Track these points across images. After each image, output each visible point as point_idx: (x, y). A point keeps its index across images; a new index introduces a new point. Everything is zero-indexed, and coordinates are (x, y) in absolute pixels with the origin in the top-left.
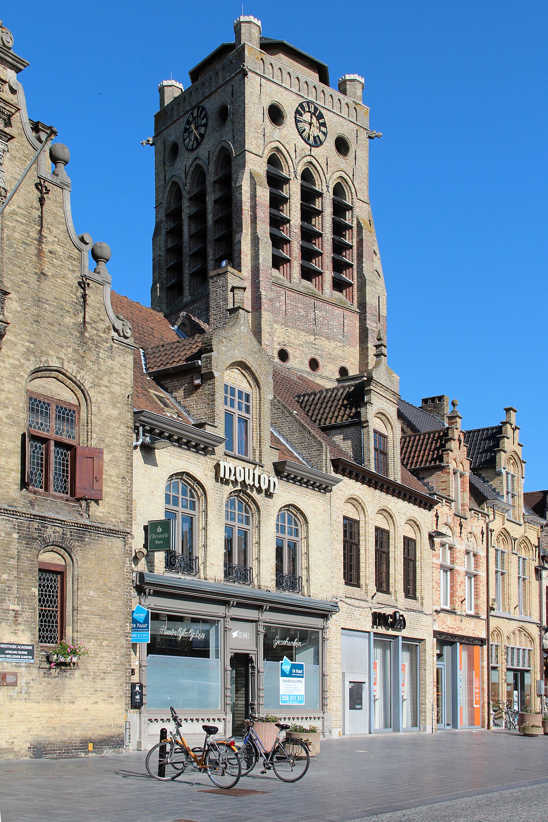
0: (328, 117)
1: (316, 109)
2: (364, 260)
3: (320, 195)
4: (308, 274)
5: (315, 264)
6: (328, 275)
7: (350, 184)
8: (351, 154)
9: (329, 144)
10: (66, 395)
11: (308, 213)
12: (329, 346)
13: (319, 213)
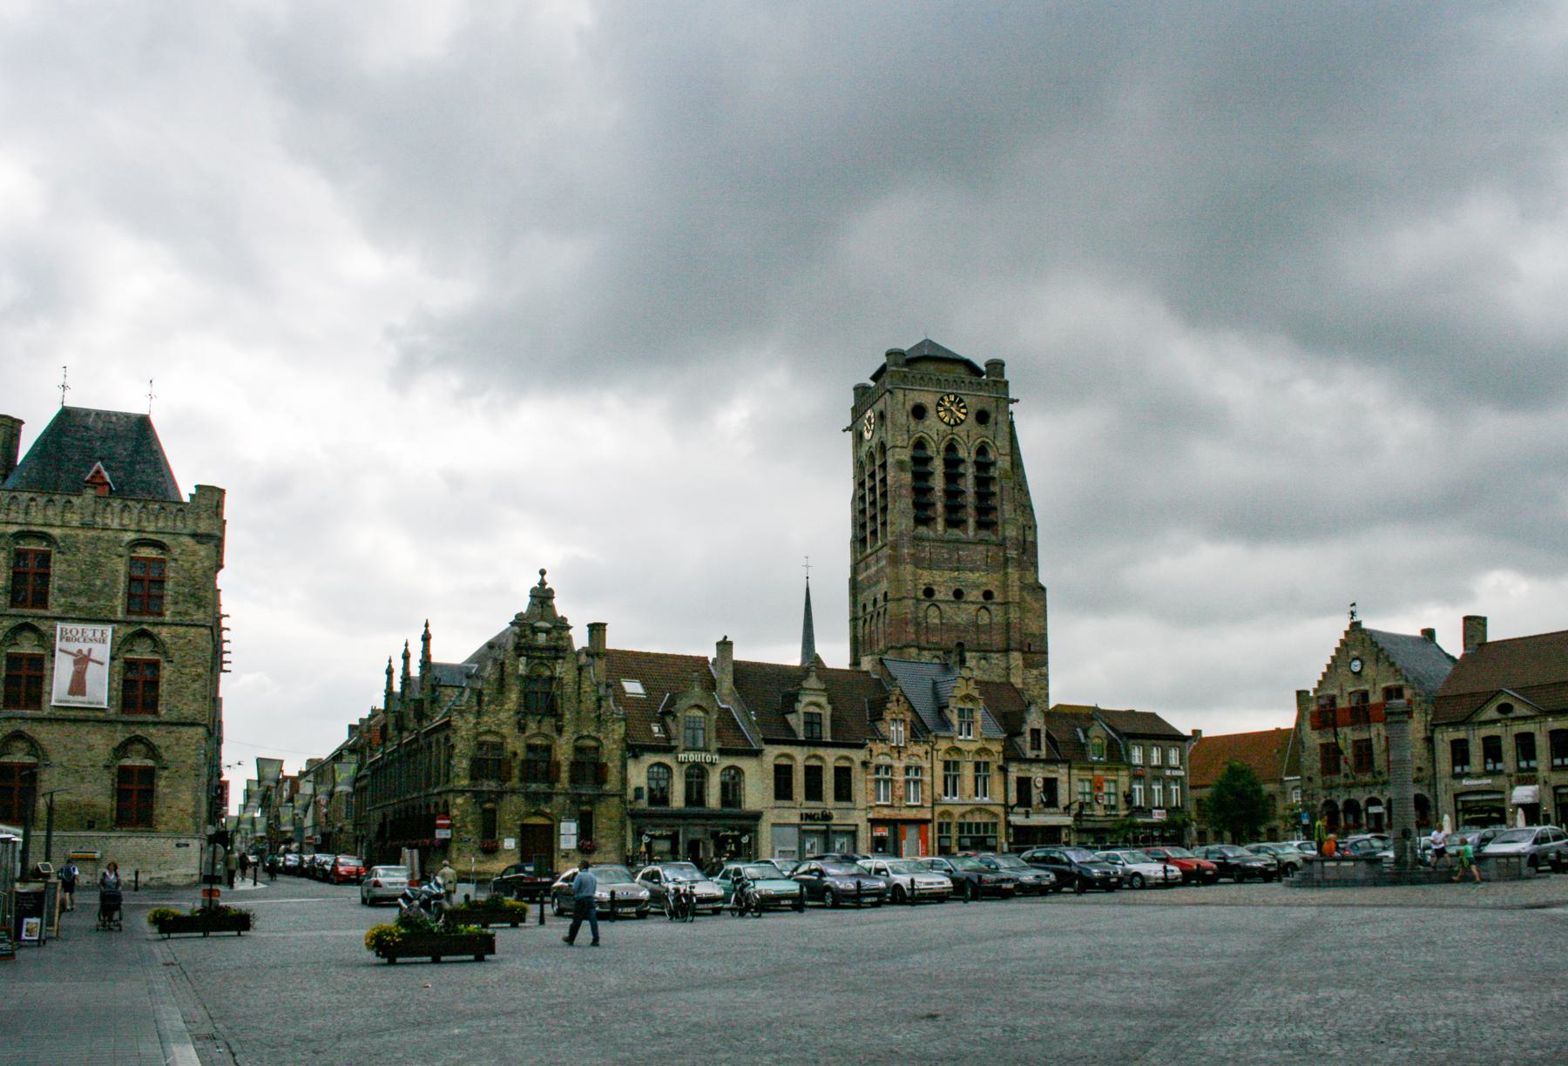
0: (967, 400)
3: (963, 461)
4: (952, 523)
5: (961, 515)
8: (992, 420)
9: (972, 418)
10: (593, 743)
11: (952, 477)
12: (973, 577)
13: (963, 475)
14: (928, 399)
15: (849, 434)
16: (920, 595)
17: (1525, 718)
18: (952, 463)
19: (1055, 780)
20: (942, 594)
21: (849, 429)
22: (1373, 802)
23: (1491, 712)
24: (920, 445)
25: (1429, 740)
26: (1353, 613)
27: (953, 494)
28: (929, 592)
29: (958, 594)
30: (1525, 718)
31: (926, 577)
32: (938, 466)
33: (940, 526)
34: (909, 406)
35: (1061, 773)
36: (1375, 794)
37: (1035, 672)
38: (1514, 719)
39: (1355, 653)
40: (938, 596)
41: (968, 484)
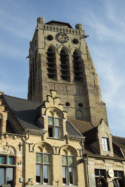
2: (85, 70)
6: (72, 77)
7: (79, 50)
14: (54, 34)
15: (28, 59)
21: (28, 57)
32: (58, 57)
33: (59, 77)
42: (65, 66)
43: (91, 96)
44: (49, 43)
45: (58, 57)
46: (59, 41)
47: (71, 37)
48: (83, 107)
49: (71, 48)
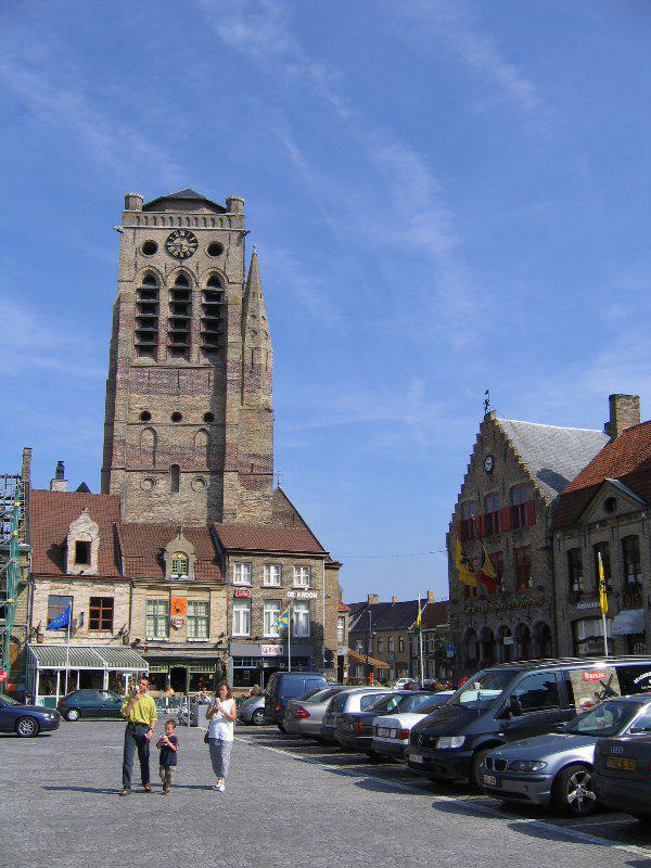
1: (186, 234)
14: (160, 237)
16: (135, 419)
17: (628, 515)
18: (181, 297)
19: (109, 602)
20: (160, 417)
22: (505, 631)
23: (599, 512)
24: (150, 278)
25: (549, 549)
26: (487, 403)
27: (181, 326)
28: (146, 416)
29: (177, 417)
30: (628, 515)
31: (140, 402)
32: (165, 298)
34: (140, 242)
35: (119, 593)
36: (506, 622)
37: (257, 494)
38: (617, 518)
39: (488, 449)
40: (154, 419)
41: (197, 314)
42: (181, 326)
43: (233, 396)
44: (145, 262)
45: (165, 298)
46: (171, 254)
47: (204, 239)
48: (214, 420)
49: (200, 271)
